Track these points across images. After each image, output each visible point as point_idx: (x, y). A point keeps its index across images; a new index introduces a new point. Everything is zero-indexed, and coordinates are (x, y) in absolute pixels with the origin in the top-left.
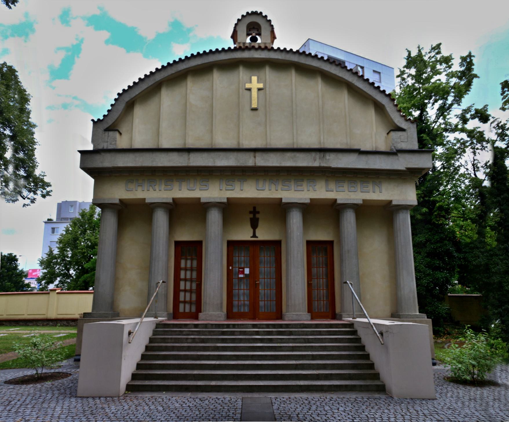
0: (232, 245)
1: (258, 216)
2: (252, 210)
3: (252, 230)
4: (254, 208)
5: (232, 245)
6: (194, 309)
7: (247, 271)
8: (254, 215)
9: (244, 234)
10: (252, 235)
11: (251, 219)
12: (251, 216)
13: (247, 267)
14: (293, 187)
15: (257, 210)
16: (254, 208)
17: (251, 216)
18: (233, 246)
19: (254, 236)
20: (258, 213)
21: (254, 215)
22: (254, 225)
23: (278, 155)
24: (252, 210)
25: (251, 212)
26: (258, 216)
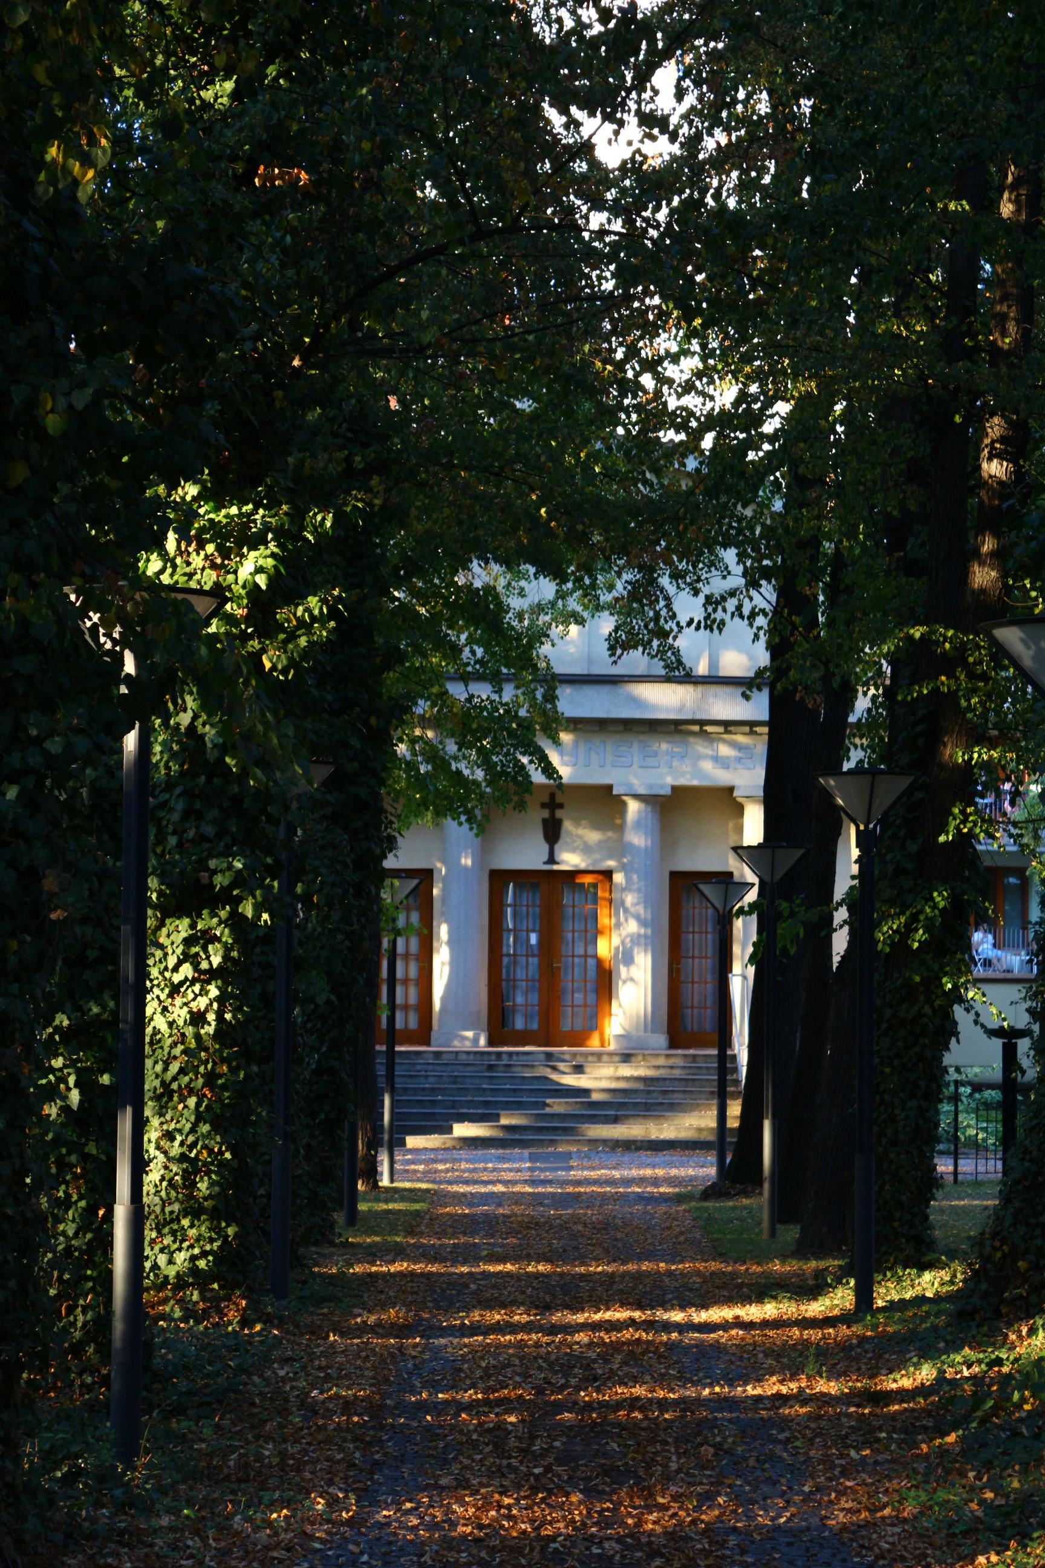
0: (499, 879)
1: (559, 814)
2: (546, 799)
3: (546, 847)
4: (552, 796)
5: (499, 879)
6: (413, 1023)
7: (534, 938)
8: (552, 813)
9: (525, 853)
10: (546, 858)
11: (545, 822)
12: (546, 814)
13: (533, 931)
14: (635, 759)
15: (559, 799)
16: (552, 796)
17: (546, 814)
18: (499, 879)
19: (552, 860)
20: (561, 806)
21: (552, 813)
22: (552, 833)
23: (604, 690)
24: (546, 799)
25: (544, 806)
26: (559, 814)
